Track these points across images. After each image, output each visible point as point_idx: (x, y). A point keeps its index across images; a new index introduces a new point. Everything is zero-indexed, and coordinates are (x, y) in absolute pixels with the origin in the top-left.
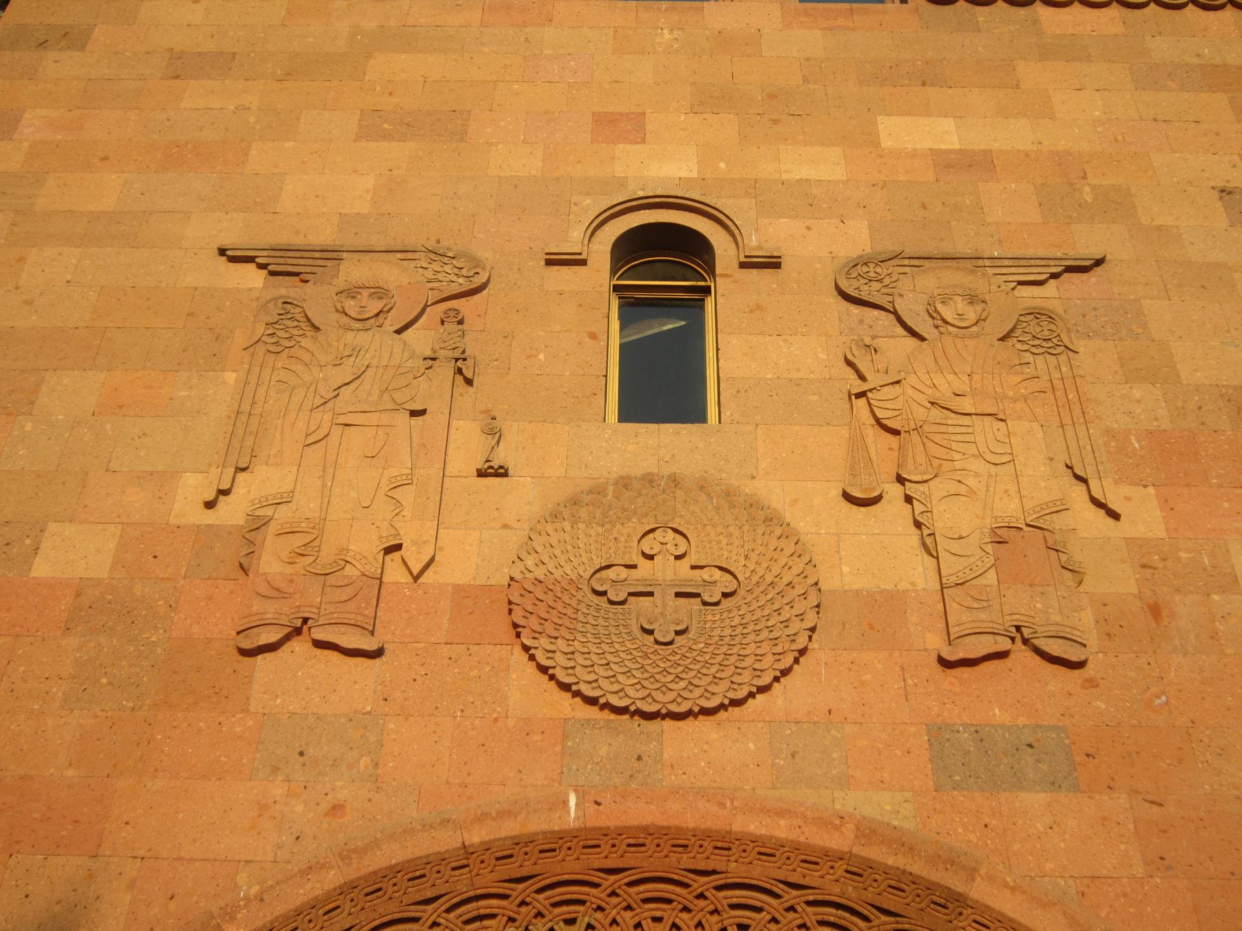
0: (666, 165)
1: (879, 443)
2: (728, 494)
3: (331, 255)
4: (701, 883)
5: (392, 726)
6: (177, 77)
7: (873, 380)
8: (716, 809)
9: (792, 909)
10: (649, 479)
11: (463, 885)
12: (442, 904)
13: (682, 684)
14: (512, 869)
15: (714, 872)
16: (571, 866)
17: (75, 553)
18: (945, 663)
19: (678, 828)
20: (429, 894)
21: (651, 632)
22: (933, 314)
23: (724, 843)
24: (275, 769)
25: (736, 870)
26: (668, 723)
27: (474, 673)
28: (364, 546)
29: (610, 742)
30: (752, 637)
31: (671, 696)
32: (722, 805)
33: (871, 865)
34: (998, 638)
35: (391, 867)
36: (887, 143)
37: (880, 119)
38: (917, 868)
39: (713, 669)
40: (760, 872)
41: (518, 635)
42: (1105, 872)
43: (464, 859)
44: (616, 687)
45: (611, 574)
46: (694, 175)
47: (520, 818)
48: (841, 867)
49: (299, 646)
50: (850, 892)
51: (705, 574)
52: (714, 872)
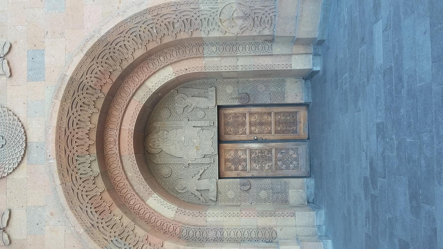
4: (68, 133)
5: (30, 204)
8: (51, 130)
9: (73, 114)
11: (70, 184)
12: (74, 188)
13: (17, 137)
14: (65, 173)
15: (65, 130)
16: (65, 161)
18: (11, 76)
19: (56, 138)
20: (72, 191)
21: (3, 145)
23: (59, 128)
24: (42, 229)
25: (65, 125)
26: (28, 141)
27: (15, 187)
29: (33, 153)
30: (4, 121)
31: (21, 140)
32: (50, 128)
33: (64, 97)
34: (4, 62)
35: (66, 200)
38: (64, 87)
39: (13, 130)
40: (65, 120)
41: (4, 177)
42: (64, 47)
43: (63, 183)
44: (19, 153)
47: (54, 173)
48: (64, 103)
50: (69, 101)
52: (65, 130)
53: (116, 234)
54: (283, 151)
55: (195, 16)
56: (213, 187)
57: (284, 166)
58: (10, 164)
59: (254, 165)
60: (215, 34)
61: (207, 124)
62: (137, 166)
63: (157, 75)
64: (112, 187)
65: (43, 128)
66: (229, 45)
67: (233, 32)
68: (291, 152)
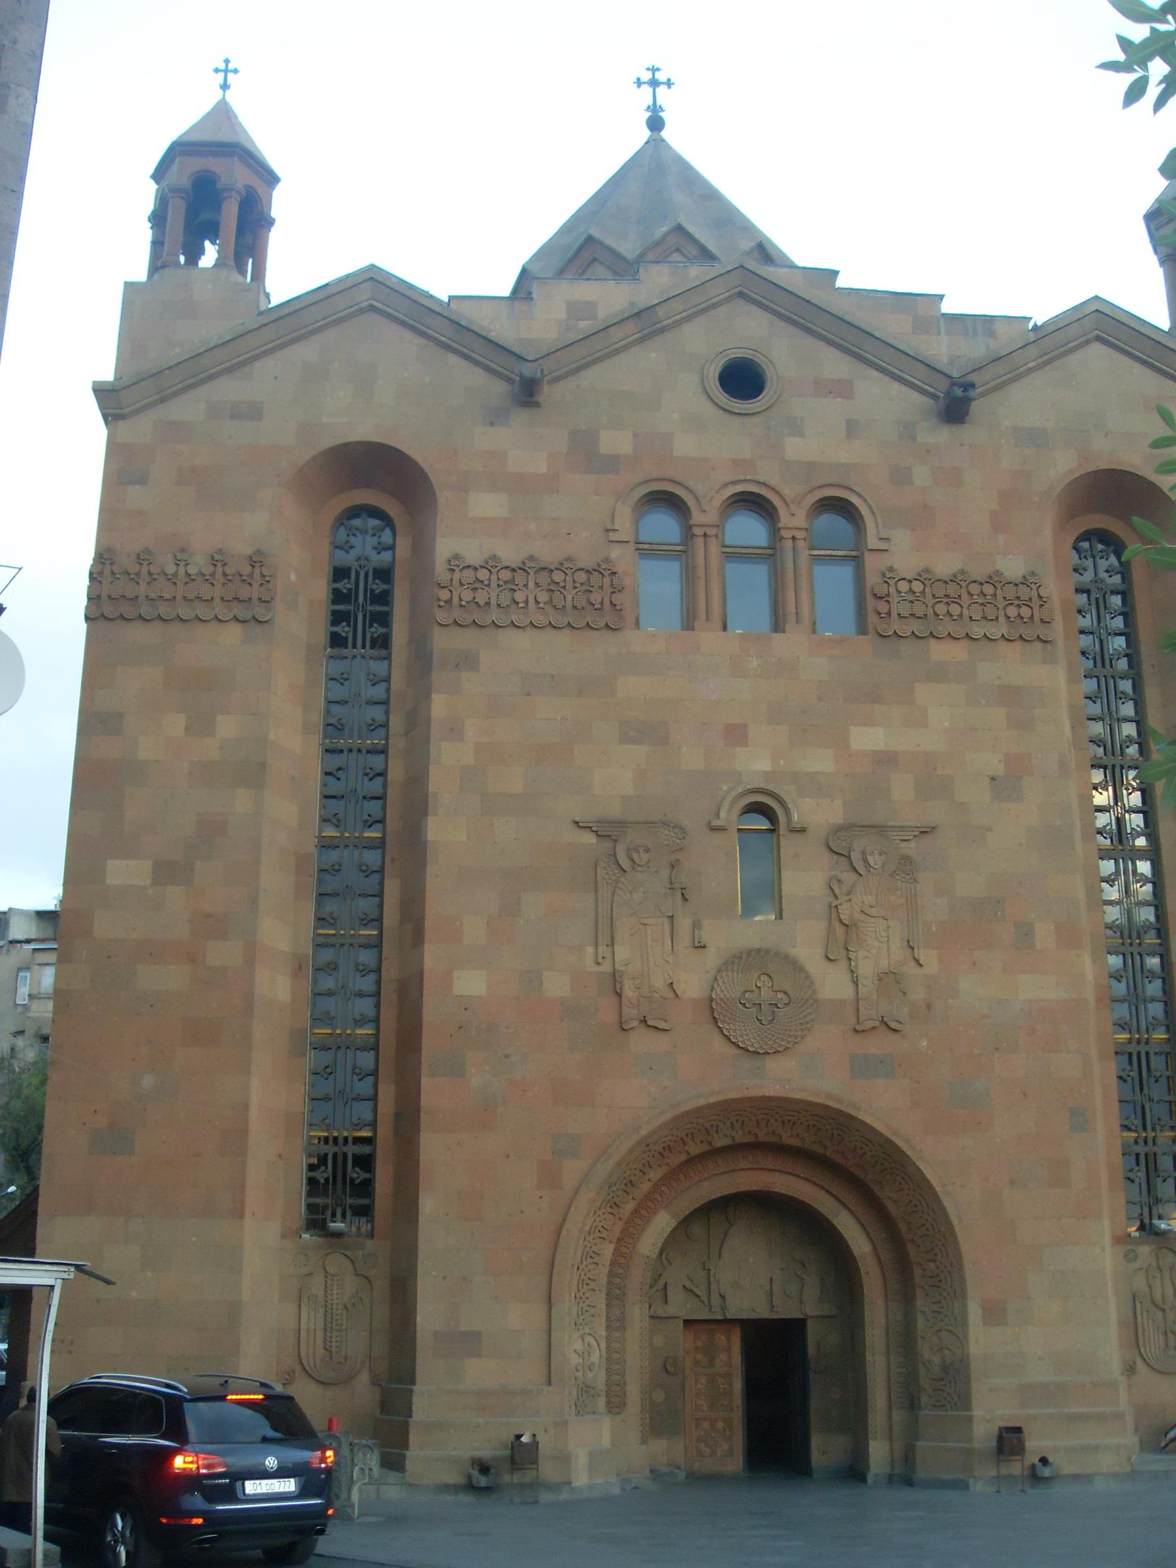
0: (756, 764)
1: (839, 930)
2: (786, 957)
3: (622, 824)
6: (529, 694)
7: (842, 899)
10: (758, 951)
17: (557, 985)
18: (856, 1031)
22: (866, 861)
23: (787, 1100)
28: (659, 983)
36: (854, 746)
37: (852, 728)
38: (843, 1108)
45: (747, 995)
46: (769, 769)
49: (643, 1025)
51: (779, 995)
53: (633, 1178)
54: (728, 1432)
55: (945, 1294)
56: (671, 1310)
57: (703, 1433)
58: (735, 1031)
59: (703, 1381)
60: (921, 1323)
61: (776, 1302)
62: (719, 1195)
63: (858, 1228)
64: (691, 1161)
65: (785, 1077)
66: (905, 1341)
67: (925, 1352)
68: (726, 1446)
